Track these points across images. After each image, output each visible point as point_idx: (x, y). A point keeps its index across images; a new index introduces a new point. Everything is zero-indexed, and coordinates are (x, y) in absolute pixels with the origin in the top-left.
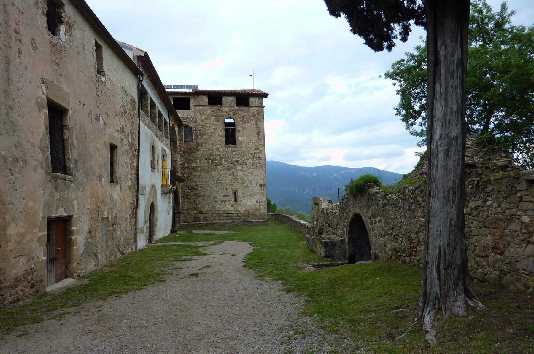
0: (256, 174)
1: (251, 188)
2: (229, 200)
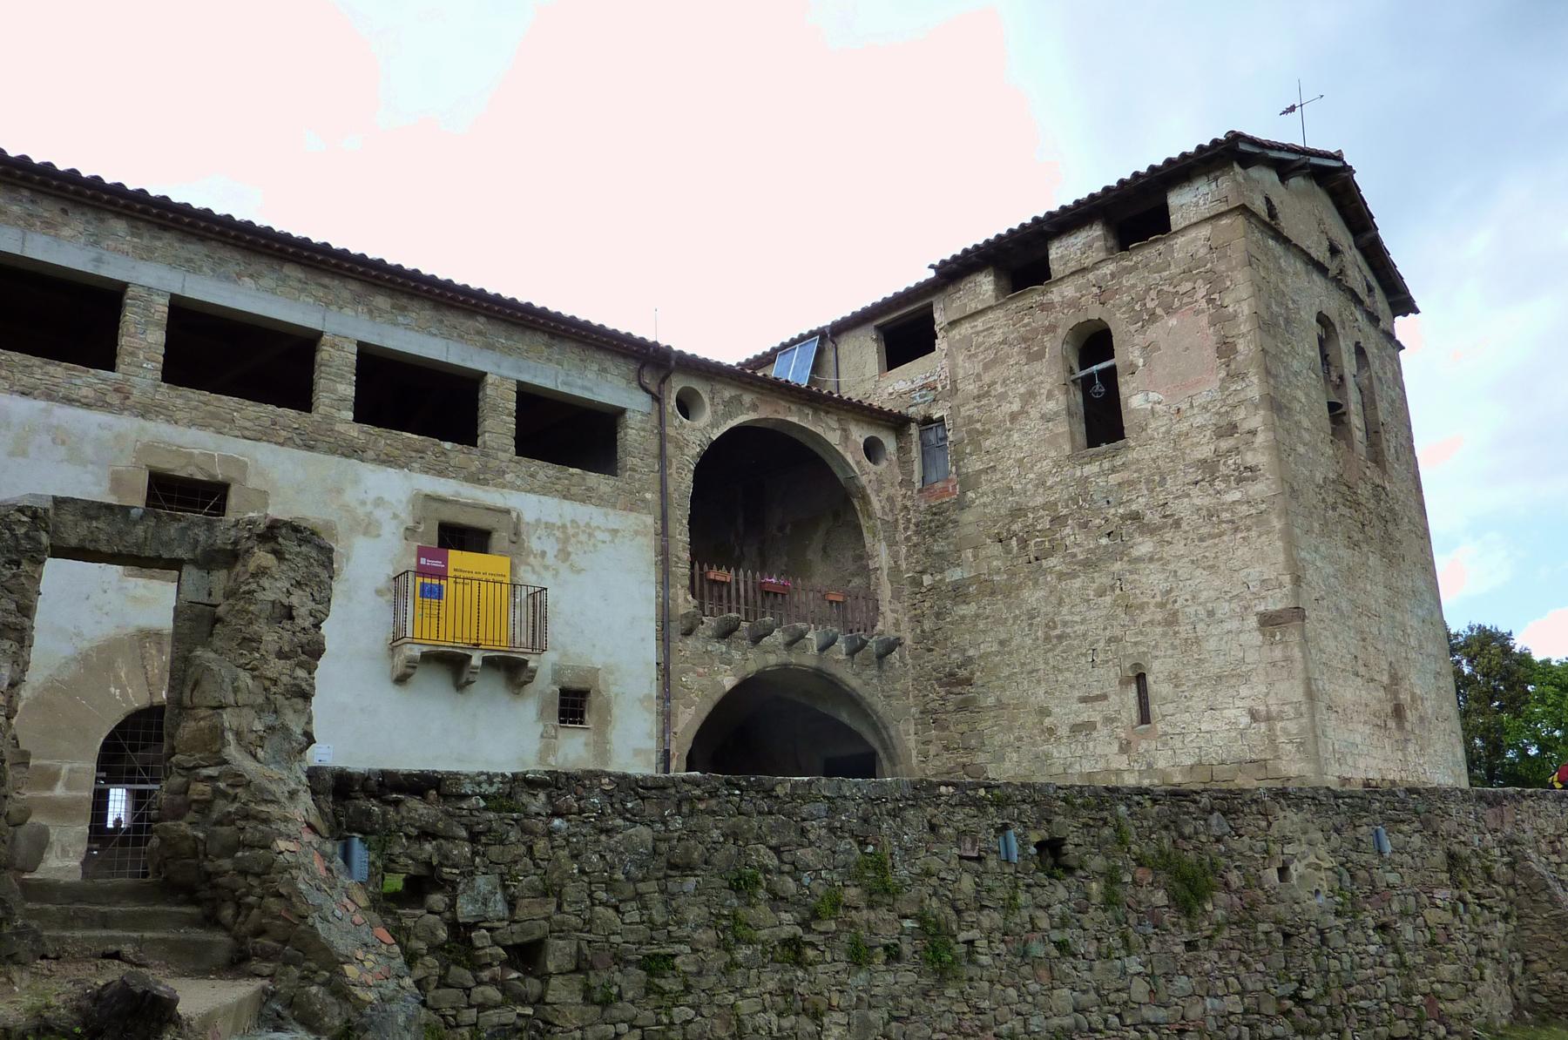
0: (1237, 564)
1: (1212, 644)
2: (1109, 720)
